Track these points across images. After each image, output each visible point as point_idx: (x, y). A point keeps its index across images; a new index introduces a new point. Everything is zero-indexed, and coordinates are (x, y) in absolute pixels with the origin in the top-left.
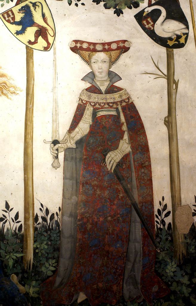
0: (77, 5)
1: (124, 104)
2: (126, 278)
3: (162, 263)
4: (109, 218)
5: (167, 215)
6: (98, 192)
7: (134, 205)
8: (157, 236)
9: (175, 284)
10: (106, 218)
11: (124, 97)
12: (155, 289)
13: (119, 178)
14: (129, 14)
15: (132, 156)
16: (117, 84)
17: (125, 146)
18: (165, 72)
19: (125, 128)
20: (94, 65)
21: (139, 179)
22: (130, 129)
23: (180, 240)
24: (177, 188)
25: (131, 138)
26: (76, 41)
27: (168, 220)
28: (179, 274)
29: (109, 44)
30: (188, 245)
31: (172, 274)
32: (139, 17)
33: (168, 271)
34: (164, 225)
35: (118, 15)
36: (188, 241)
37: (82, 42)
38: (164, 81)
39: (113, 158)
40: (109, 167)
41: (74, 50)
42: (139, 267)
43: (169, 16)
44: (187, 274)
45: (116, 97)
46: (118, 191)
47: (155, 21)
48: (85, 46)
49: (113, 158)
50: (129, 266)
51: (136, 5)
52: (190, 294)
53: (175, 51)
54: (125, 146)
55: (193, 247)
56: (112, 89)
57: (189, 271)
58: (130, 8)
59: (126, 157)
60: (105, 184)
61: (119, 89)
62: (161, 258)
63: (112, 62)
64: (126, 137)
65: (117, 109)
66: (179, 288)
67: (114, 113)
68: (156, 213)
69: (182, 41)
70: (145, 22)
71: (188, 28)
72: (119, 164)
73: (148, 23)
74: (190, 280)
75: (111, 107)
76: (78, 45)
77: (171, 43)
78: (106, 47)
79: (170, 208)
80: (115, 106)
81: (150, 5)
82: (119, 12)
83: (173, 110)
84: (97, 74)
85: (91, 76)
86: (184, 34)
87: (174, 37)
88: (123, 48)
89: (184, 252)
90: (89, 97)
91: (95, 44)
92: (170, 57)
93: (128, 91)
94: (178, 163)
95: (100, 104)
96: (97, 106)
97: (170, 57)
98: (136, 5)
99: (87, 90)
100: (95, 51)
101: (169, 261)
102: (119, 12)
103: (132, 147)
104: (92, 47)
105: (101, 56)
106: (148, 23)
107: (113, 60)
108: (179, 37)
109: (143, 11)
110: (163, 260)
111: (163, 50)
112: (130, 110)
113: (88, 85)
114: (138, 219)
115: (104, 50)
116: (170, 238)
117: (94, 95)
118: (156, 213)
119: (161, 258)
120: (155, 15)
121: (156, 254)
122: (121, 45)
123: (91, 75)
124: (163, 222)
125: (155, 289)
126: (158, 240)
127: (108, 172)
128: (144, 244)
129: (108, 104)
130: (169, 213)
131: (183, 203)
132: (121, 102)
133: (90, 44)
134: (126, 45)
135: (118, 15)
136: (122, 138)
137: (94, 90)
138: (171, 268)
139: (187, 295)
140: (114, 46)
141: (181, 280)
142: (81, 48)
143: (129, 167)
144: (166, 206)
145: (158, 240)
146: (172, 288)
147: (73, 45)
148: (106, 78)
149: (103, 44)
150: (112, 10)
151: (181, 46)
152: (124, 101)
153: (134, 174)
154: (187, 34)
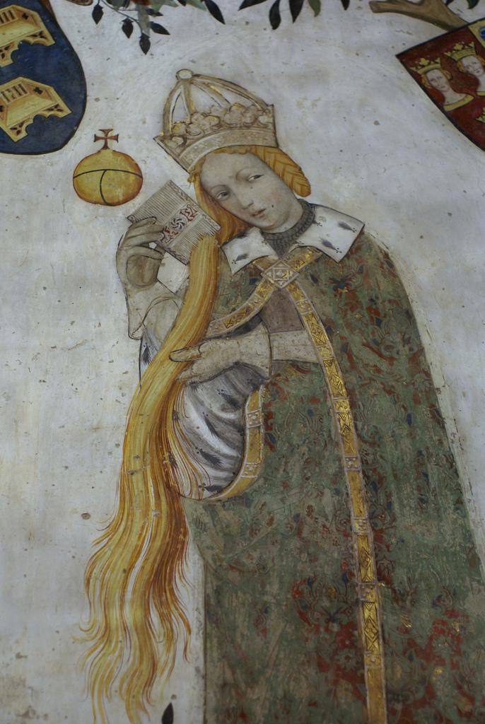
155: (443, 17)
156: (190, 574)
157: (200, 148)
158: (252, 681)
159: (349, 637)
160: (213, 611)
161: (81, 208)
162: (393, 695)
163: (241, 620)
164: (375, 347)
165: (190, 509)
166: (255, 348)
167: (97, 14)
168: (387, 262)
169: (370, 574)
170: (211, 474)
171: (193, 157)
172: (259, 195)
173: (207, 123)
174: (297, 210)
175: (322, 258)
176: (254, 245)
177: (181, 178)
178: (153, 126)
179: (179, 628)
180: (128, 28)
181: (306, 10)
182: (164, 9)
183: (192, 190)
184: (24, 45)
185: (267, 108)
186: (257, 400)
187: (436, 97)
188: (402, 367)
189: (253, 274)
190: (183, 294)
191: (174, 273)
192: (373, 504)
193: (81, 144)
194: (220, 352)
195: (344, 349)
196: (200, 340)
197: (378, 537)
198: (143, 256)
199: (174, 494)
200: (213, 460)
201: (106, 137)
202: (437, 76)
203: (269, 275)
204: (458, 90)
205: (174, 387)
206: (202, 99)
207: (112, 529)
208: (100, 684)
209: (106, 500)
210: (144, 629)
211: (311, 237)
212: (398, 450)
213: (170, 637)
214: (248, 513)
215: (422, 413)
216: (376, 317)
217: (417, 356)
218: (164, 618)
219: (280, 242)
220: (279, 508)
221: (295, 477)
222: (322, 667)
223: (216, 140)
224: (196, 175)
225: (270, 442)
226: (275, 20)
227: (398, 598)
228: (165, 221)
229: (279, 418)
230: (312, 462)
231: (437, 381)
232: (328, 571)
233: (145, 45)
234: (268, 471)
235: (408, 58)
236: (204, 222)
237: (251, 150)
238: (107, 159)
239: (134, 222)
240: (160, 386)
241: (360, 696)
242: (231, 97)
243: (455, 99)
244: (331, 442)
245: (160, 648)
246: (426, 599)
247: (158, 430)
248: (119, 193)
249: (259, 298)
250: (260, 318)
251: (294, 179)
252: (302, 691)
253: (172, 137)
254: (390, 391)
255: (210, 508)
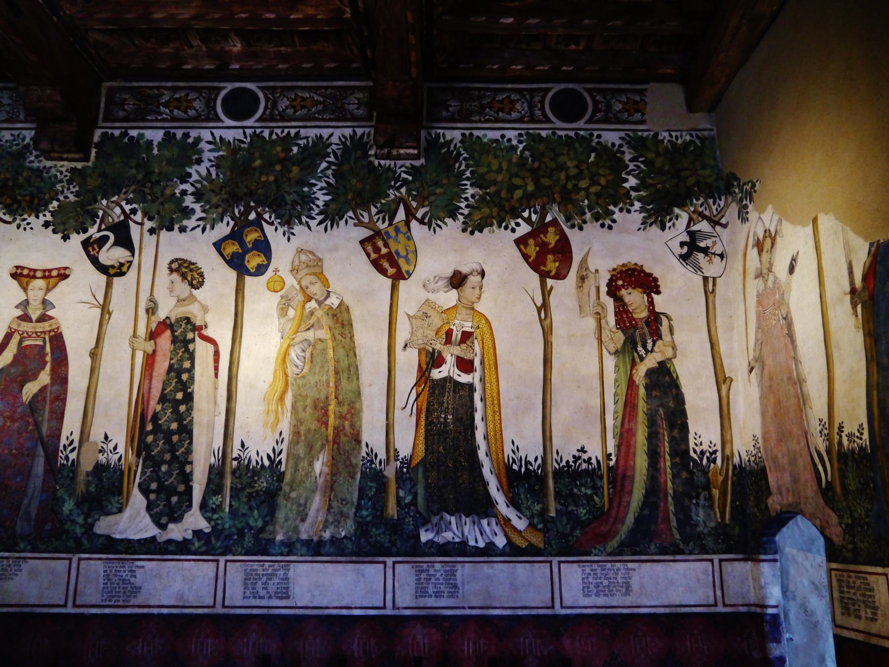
0: (25, 229)
1: (53, 333)
2: (21, 512)
3: (60, 501)
4: (14, 451)
5: (72, 451)
6: (9, 424)
7: (41, 438)
8: (59, 472)
9: (69, 523)
10: (10, 450)
11: (54, 327)
12: (48, 527)
13: (31, 410)
14: (76, 240)
15: (49, 388)
16: (49, 313)
17: (44, 378)
18: (101, 303)
19: (48, 358)
20: (30, 292)
21: (52, 411)
22: (54, 360)
23: (82, 477)
24: (88, 423)
25: (53, 369)
26: (17, 267)
27: (73, 456)
28: (75, 512)
29: (50, 271)
30: (88, 484)
31: (68, 512)
32: (86, 244)
33: (64, 509)
34: (68, 461)
35: (65, 241)
36: (90, 478)
37: (23, 268)
38: (99, 311)
39: (30, 389)
40: (24, 399)
41: (14, 276)
42: (35, 504)
43: (117, 243)
44: (83, 513)
45: (46, 326)
46: (28, 423)
47: (100, 248)
48: (25, 272)
49: (30, 389)
50: (26, 502)
51: (85, 231)
52: (83, 534)
53: (116, 279)
54: (44, 378)
55: (94, 485)
56: (43, 318)
57: (86, 510)
58: (78, 233)
59: (43, 389)
60: (17, 415)
61: (51, 318)
62: (59, 495)
63: (48, 290)
64: (48, 367)
65: (44, 338)
66: (73, 527)
67: (40, 343)
68: (61, 448)
69: (124, 269)
70: (90, 249)
71: (133, 255)
72: (35, 396)
73: (94, 249)
74: (85, 519)
75: (39, 336)
76: (19, 271)
77: (112, 271)
78: (47, 274)
79: (76, 444)
80: (43, 335)
81: (99, 230)
82: (66, 238)
83: (101, 341)
84: (31, 301)
85: (25, 304)
86: (128, 262)
87: (117, 265)
88: (63, 275)
89: (84, 490)
90: (19, 325)
91: (35, 271)
92: (109, 285)
93: (60, 320)
94: (95, 397)
95: (27, 333)
96: (25, 335)
97: (109, 285)
98: (85, 231)
99: (18, 318)
100: (34, 277)
101: (67, 498)
102: (66, 238)
103: (52, 379)
104: (32, 274)
105: (40, 283)
106: (94, 249)
107: (50, 286)
108: (122, 265)
109: (91, 237)
110: (61, 497)
111: (104, 278)
112: (58, 341)
113: (19, 312)
114: (42, 453)
115: (44, 277)
116: (71, 475)
117: (24, 323)
118: (61, 448)
119: (59, 495)
120: (103, 240)
121: (56, 490)
122: (62, 272)
123: (25, 303)
124: (67, 458)
125: (48, 527)
126: (59, 476)
127: (23, 404)
128: (44, 480)
129: (36, 333)
130: (75, 448)
131: (92, 439)
132: (50, 331)
133: (30, 270)
134: (67, 272)
135: (65, 241)
136: (43, 368)
137: (25, 318)
138: (68, 506)
139: (79, 535)
140: (54, 273)
141: (76, 519)
142: (21, 275)
143: (44, 399)
144: (72, 442)
145: (59, 476)
146: (66, 527)
147: (14, 270)
148: (41, 306)
149: (44, 271)
150: (60, 235)
151: (122, 274)
152: (53, 330)
153: (47, 407)
154: (131, 262)
155: (374, 228)
156: (289, 397)
157: (302, 273)
158: (301, 424)
159: (326, 414)
160: (294, 407)
161: (269, 294)
162: (335, 428)
163: (300, 409)
164: (341, 334)
165: (290, 380)
166: (310, 335)
167: (276, 229)
168: (348, 309)
169: (333, 397)
170: (296, 371)
171: (299, 277)
172: (316, 289)
173: (304, 266)
174: (326, 293)
175: (331, 308)
176: (313, 304)
177: (295, 283)
178: (289, 267)
179: (285, 411)
180: (284, 234)
181: (335, 226)
182: (295, 227)
183: (298, 287)
184: (256, 240)
185: (320, 260)
186: (310, 349)
187: (368, 255)
188: (348, 340)
189: (312, 313)
190: (293, 319)
191: (291, 313)
192: (336, 378)
193: (269, 273)
194: (302, 336)
195: (333, 335)
196: (297, 332)
197: (336, 387)
198: (283, 310)
199: (286, 376)
200: (297, 367)
201: (276, 271)
202: (370, 248)
203: (316, 313)
204: (375, 253)
205: (289, 346)
206: (303, 257)
207: (271, 385)
208: (266, 425)
209: (269, 377)
210: (277, 412)
211: (328, 302)
212: (344, 364)
213: (283, 413)
214: (305, 381)
215: (352, 353)
216: (343, 326)
217: (352, 338)
218: (282, 408)
219: (320, 303)
220: (312, 380)
221: (317, 371)
222: (318, 421)
223: (306, 271)
224: (299, 282)
225: (312, 362)
226: (326, 230)
227: (339, 403)
228: (290, 297)
229: (314, 355)
230: (322, 367)
231: (356, 344)
232: (322, 396)
233: (289, 239)
234: (311, 369)
235: (362, 242)
236: (300, 297)
237: (315, 274)
238: (276, 278)
239: (282, 297)
240: (285, 345)
241: (327, 429)
242: (311, 257)
243: (374, 256)
244: (327, 361)
245: (280, 416)
246: (346, 404)
247: (284, 357)
248: (278, 288)
249: (312, 321)
250: (312, 326)
251: (325, 283)
252: (313, 427)
253: (294, 270)
254: (343, 347)
255: (295, 380)
